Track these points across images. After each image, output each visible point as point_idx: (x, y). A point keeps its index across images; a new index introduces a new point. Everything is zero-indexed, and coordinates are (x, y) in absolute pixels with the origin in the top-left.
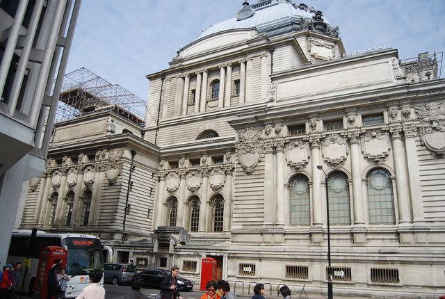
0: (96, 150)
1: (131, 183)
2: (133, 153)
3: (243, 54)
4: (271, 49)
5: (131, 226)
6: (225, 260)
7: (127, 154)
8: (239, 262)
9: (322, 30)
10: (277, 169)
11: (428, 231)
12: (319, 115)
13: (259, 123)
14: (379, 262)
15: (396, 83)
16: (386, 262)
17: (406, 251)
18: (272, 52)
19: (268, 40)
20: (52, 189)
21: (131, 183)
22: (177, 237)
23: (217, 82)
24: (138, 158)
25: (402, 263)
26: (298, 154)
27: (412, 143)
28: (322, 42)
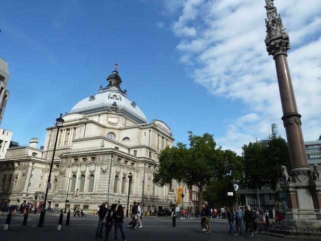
0: (20, 162)
1: (31, 175)
2: (33, 164)
3: (77, 124)
4: (85, 123)
5: (31, 191)
6: (52, 203)
7: (31, 164)
8: (55, 203)
9: (115, 111)
10: (69, 174)
11: (97, 194)
12: (81, 156)
13: (66, 157)
14: (85, 203)
15: (100, 148)
16: (87, 203)
17: (92, 200)
18: (86, 125)
19: (87, 119)
20: (3, 176)
21: (31, 175)
22: (40, 195)
23: (69, 133)
24: (36, 165)
25: (90, 203)
26: (75, 169)
27: (99, 167)
28: (113, 116)
